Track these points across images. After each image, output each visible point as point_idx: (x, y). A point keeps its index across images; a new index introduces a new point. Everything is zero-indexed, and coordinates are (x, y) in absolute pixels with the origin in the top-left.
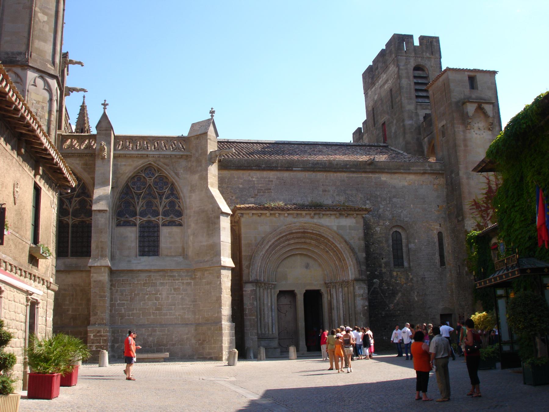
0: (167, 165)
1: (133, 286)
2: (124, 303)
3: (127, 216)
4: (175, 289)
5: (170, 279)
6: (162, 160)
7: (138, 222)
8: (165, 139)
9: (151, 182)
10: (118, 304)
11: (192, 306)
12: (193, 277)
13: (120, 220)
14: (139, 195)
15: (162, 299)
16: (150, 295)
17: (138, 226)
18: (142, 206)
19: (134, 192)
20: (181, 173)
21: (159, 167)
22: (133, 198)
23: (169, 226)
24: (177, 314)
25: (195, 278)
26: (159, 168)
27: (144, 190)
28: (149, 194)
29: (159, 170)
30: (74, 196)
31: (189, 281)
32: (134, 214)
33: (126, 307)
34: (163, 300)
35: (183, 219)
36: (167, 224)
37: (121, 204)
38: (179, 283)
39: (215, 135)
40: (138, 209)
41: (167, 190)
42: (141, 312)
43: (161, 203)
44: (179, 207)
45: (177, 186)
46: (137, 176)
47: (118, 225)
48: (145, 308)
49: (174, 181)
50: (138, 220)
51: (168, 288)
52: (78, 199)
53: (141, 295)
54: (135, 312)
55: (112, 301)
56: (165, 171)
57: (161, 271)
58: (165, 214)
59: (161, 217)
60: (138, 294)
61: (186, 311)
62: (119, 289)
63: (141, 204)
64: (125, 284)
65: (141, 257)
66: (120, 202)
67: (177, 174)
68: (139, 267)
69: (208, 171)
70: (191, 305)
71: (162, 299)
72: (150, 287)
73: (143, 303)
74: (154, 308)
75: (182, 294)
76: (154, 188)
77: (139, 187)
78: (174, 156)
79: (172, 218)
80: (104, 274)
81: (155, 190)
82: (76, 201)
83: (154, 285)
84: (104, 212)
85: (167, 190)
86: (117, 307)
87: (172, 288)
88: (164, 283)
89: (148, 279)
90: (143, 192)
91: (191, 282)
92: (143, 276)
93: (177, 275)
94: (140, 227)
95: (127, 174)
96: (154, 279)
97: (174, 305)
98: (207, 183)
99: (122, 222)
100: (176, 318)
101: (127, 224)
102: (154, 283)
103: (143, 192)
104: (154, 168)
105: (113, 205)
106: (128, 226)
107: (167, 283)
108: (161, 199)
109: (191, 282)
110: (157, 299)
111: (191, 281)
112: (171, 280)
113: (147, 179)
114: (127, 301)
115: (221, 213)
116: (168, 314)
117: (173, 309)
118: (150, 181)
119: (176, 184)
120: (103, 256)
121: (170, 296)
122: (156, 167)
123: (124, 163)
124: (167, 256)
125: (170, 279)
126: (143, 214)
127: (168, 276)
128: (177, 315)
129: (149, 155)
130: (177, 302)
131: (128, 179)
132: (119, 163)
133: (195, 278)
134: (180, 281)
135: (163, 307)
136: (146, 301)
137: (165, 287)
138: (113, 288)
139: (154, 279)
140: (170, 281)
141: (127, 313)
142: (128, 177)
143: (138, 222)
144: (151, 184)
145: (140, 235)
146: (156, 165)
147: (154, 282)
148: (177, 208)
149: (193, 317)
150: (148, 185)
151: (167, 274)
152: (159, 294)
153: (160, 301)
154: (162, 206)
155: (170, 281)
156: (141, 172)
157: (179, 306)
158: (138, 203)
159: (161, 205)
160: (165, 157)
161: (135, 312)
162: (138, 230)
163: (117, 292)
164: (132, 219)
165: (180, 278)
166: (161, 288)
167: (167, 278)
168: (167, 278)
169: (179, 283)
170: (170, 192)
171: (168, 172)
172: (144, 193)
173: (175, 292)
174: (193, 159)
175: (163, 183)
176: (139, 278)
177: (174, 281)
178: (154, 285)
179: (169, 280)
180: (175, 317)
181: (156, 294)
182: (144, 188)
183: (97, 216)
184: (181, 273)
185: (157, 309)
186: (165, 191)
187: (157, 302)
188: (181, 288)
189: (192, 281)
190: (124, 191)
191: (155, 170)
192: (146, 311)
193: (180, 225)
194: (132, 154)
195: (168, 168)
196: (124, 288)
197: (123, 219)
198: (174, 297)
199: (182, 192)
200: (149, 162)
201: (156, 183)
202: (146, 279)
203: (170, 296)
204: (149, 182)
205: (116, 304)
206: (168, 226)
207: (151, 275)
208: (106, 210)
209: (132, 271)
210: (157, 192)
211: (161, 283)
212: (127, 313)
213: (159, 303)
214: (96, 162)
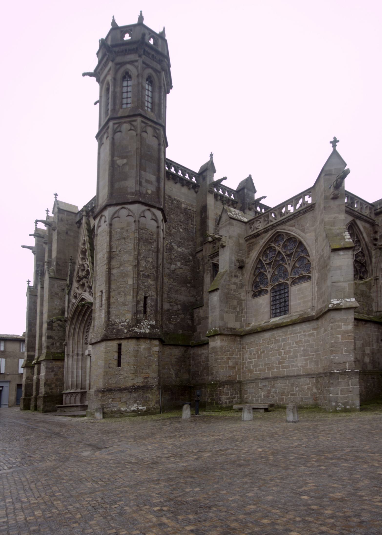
24: (299, 365)
83: (278, 341)
100: (298, 369)
102: (277, 340)
117: (295, 361)
121: (292, 350)
147: (277, 339)
152: (281, 349)
178: (278, 341)
202: (270, 338)
211: (283, 339)
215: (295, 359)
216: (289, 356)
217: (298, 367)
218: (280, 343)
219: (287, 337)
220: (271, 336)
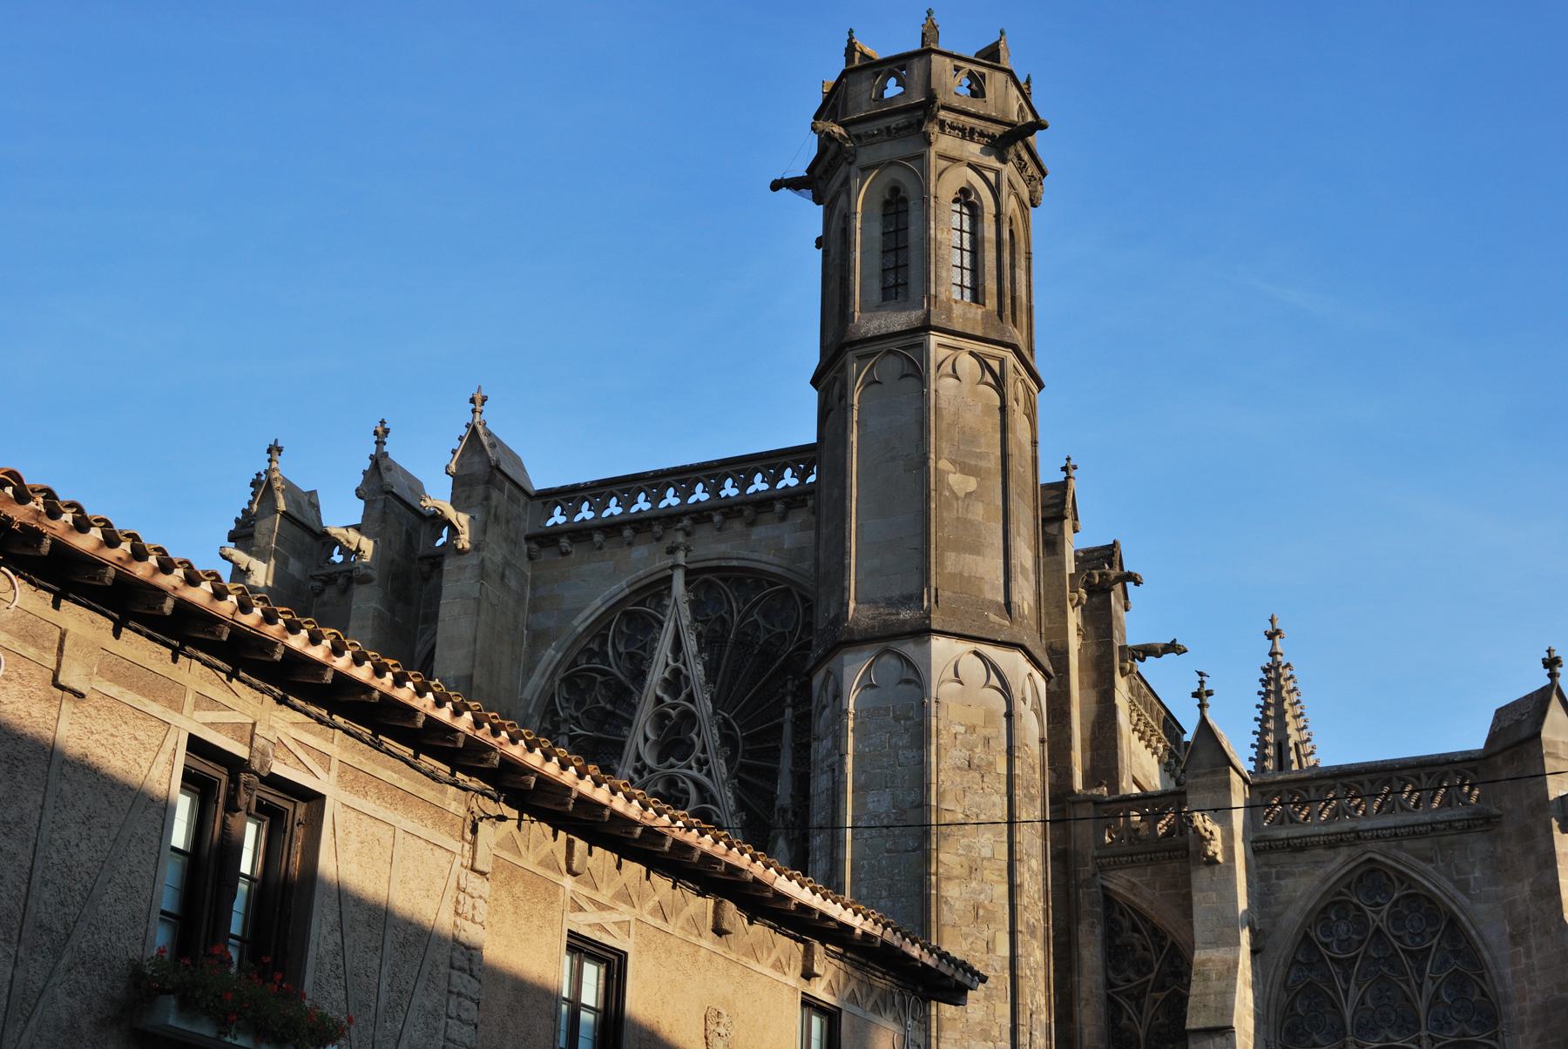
0: (1430, 860)
9: (1382, 921)
18: (1362, 1001)
19: (1332, 959)
20: (1475, 878)
22: (1330, 980)
26: (1401, 872)
27: (1362, 949)
29: (1403, 878)
30: (1149, 989)
37: (1293, 999)
40: (1348, 1013)
41: (1435, 941)
43: (1420, 986)
44: (1483, 994)
45: (1468, 925)
46: (1334, 903)
49: (1454, 907)
52: (1161, 996)
66: (1288, 996)
76: (1392, 939)
77: (1347, 940)
79: (1464, 1036)
81: (1397, 944)
82: (1155, 1002)
85: (1435, 941)
90: (1356, 957)
103: (1356, 957)
105: (1268, 1006)
113: (1367, 909)
119: (1463, 918)
131: (1307, 916)
144: (1381, 924)
150: (1371, 930)
154: (1424, 999)
158: (1346, 992)
159: (1421, 996)
171: (1431, 882)
182: (1361, 942)
186: (1431, 947)
190: (1300, 957)
195: (1430, 867)
201: (1396, 918)
204: (1374, 921)
210: (1403, 950)
214: (1193, 875)
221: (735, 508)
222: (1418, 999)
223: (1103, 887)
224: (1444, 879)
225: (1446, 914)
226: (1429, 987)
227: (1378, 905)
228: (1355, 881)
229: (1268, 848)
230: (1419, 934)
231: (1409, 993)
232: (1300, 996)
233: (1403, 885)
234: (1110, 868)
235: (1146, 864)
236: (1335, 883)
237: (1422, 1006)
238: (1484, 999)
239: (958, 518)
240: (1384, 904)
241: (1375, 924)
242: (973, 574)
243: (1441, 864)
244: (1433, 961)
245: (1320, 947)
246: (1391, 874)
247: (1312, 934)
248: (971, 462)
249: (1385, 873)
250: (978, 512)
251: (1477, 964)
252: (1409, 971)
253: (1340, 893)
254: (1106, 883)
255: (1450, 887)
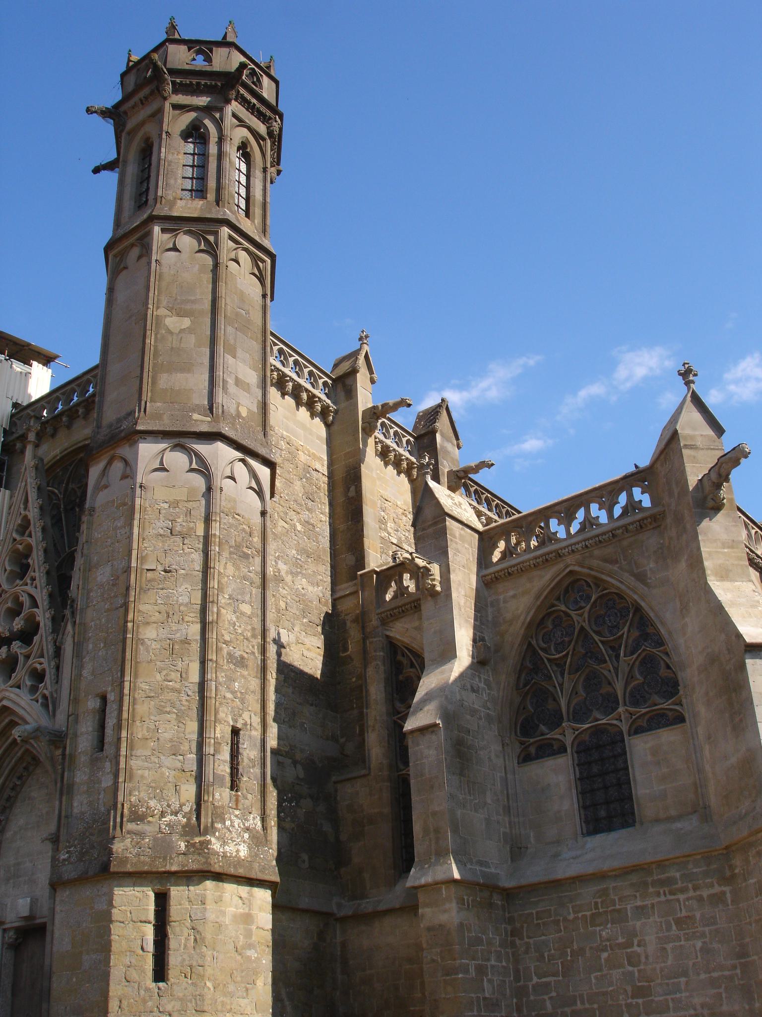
0: (614, 562)
1: (565, 928)
2: (549, 983)
3: (543, 728)
4: (679, 922)
5: (662, 892)
6: (597, 552)
7: (569, 740)
8: (593, 494)
10: (533, 986)
11: (738, 971)
12: (728, 874)
13: (527, 744)
14: (559, 664)
15: (647, 957)
16: (612, 949)
17: (569, 750)
18: (575, 692)
19: (549, 660)
21: (593, 573)
23: (650, 730)
24: (697, 1001)
25: (733, 877)
26: (595, 578)
28: (587, 653)
29: (598, 582)
31: (717, 889)
32: (556, 720)
33: (554, 994)
34: (651, 960)
35: (684, 701)
36: (645, 725)
38: (688, 899)
39: (710, 432)
42: (595, 1006)
43: (616, 669)
44: (668, 667)
46: (549, 615)
47: (526, 758)
48: (605, 994)
49: (636, 597)
50: (568, 734)
51: (658, 920)
53: (588, 954)
54: (579, 1006)
55: (519, 981)
56: (609, 579)
57: (633, 871)
58: (637, 698)
59: (621, 709)
60: (582, 951)
61: (722, 990)
62: (531, 941)
63: (568, 686)
64: (544, 924)
65: (588, 839)
67: (641, 578)
68: (574, 870)
69: (700, 538)
70: (734, 967)
71: (647, 957)
72: (609, 926)
73: (596, 978)
74: (629, 989)
75: (703, 935)
78: (621, 531)
80: (447, 906)
81: (596, 638)
84: (433, 732)
85: (626, 629)
86: (532, 998)
87: (671, 918)
88: (646, 906)
89: (602, 902)
90: (568, 653)
91: (723, 893)
92: (587, 893)
93: (678, 875)
94: (577, 752)
95: (522, 618)
96: (616, 898)
97: (685, 974)
98: (703, 570)
99: (533, 750)
101: (549, 750)
102: (619, 911)
103: (568, 653)
104: (586, 581)
106: (549, 755)
107: (653, 905)
108: (617, 657)
109: (723, 893)
110: (633, 960)
111: (724, 888)
112: (665, 894)
113: (572, 613)
114: (555, 974)
115: (746, 651)
116: (671, 1005)
117: (683, 987)
118: (580, 618)
119: (643, 604)
120: (441, 854)
121: (669, 946)
122: (589, 575)
123: (511, 593)
124: (657, 821)
125: (662, 892)
126: (579, 715)
127: (654, 884)
128: (698, 1007)
129: (561, 549)
130: (691, 963)
132: (501, 597)
133: (733, 877)
134: (691, 893)
135: (652, 984)
136: (605, 972)
137: (651, 919)
138: (518, 942)
139: (616, 898)
140: (663, 898)
141: (559, 1011)
142: (526, 625)
143: (569, 740)
144: (584, 624)
145: (581, 773)
146: (585, 571)
147: (618, 907)
148: (663, 672)
149: (747, 1007)
151: (650, 880)
153: (642, 967)
155: (663, 898)
156: (556, 603)
157: (698, 974)
158: (561, 685)
160: (600, 542)
161: (579, 1006)
162: (570, 762)
163: (527, 952)
164: (555, 735)
165: (690, 886)
166: (638, 924)
167: (651, 890)
168: (651, 890)
169: (688, 899)
170: (636, 633)
171: (617, 580)
172: (573, 655)
173: (682, 932)
174: (669, 520)
175: (616, 614)
176: (578, 903)
177: (672, 897)
179: (658, 894)
180: (692, 1012)
181: (629, 944)
183: (418, 745)
184: (690, 866)
185: (640, 992)
186: (623, 634)
187: (636, 969)
188: (698, 915)
189: (727, 889)
191: (589, 585)
192: (610, 1002)
193: (680, 719)
194: (523, 562)
196: (543, 937)
197: (532, 740)
198: (681, 946)
199: (662, 623)
200: (568, 570)
202: (596, 903)
203: (669, 946)
205: (530, 986)
206: (650, 729)
207: (607, 889)
208: (435, 725)
209: (556, 884)
210: (602, 642)
211: (637, 908)
212: (559, 1011)
213: (639, 971)
215: (683, 980)
216: (662, 970)
217: (695, 1009)
218: (631, 923)
219: (648, 902)
220: (600, 897)
221: (90, 400)
222: (616, 680)
223: (387, 637)
224: (626, 574)
225: (633, 605)
226: (624, 668)
227: (581, 608)
228: (562, 593)
229: (494, 579)
230: (616, 626)
231: (609, 678)
232: (529, 697)
233: (599, 587)
234: (389, 620)
235: (412, 612)
236: (546, 597)
237: (619, 687)
238: (669, 671)
239: (172, 348)
240: (584, 607)
241: (580, 625)
242: (183, 387)
243: (624, 563)
244: (626, 647)
245: (540, 651)
246: (589, 580)
247: (534, 642)
248: (186, 307)
249: (584, 580)
250: (190, 341)
251: (660, 642)
252: (607, 659)
253: (553, 606)
254: (388, 633)
255: (631, 581)
